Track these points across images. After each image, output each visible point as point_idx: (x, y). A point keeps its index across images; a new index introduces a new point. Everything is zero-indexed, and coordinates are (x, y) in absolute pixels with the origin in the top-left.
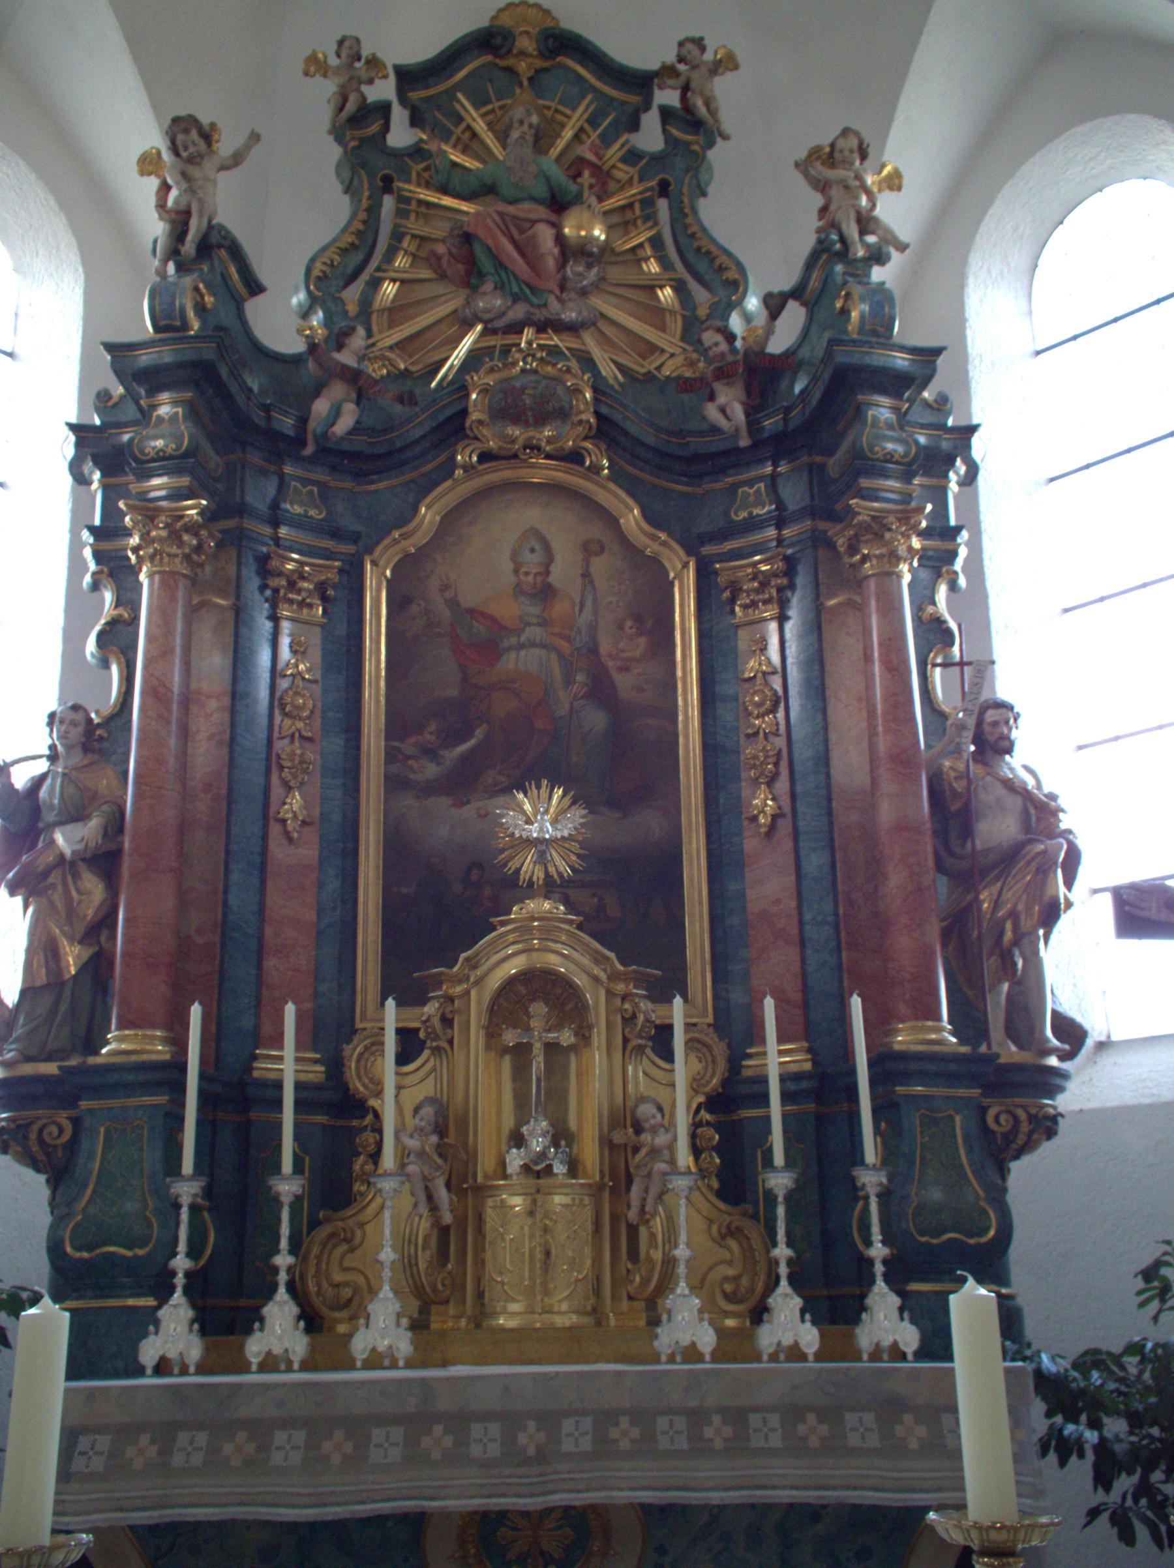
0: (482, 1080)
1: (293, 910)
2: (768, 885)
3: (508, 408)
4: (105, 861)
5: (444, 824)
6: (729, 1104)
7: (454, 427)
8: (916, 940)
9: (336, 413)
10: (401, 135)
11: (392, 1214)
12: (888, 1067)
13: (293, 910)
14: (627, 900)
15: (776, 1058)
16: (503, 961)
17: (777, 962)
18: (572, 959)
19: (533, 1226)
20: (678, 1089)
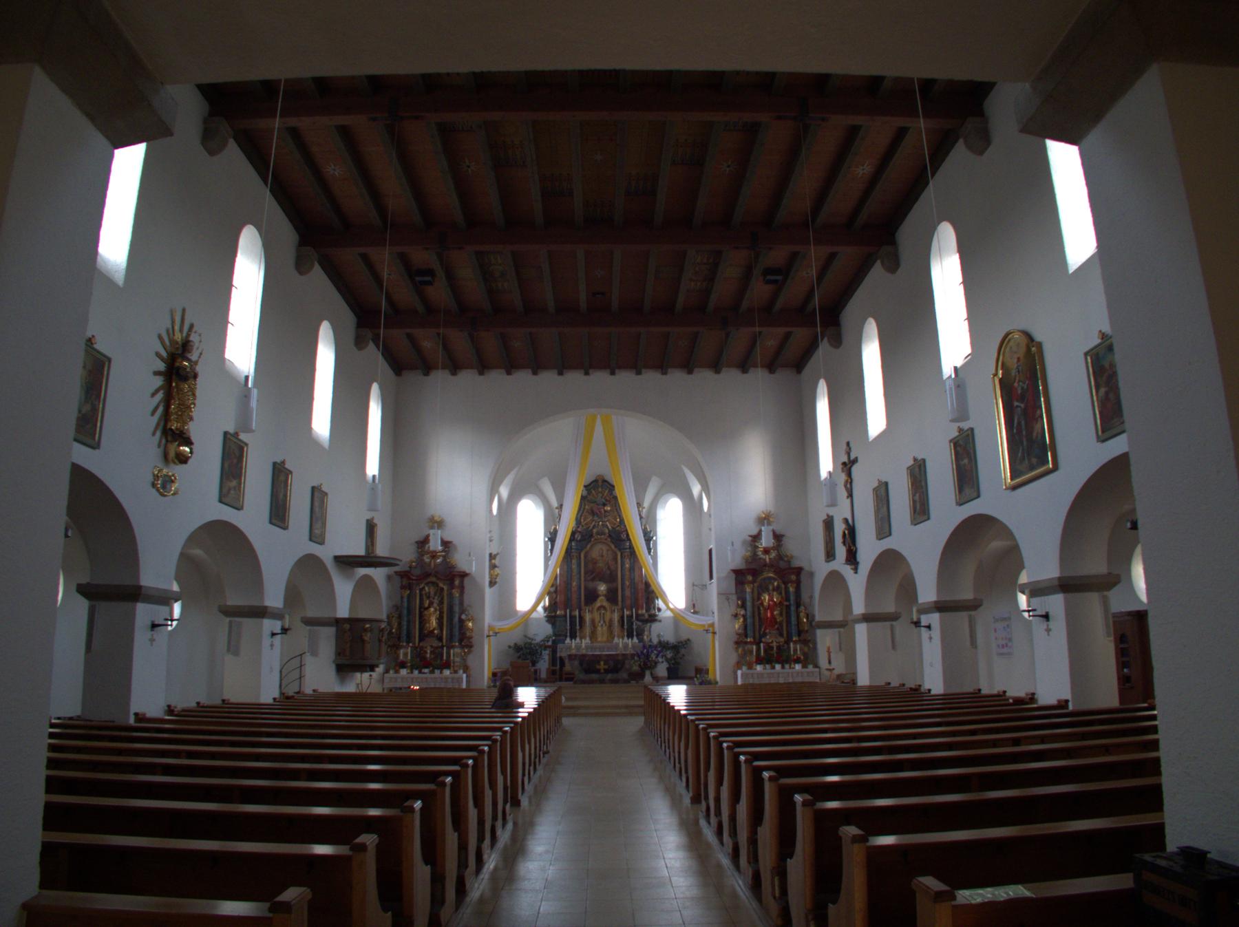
0: (596, 616)
1: (575, 596)
2: (628, 593)
3: (598, 533)
4: (556, 592)
5: (591, 585)
6: (622, 617)
7: (592, 536)
8: (642, 601)
9: (578, 537)
10: (585, 493)
11: (588, 630)
12: (637, 615)
13: (575, 596)
14: (612, 597)
15: (626, 613)
16: (598, 604)
17: (628, 602)
18: (605, 604)
19: (601, 630)
20: (616, 616)
